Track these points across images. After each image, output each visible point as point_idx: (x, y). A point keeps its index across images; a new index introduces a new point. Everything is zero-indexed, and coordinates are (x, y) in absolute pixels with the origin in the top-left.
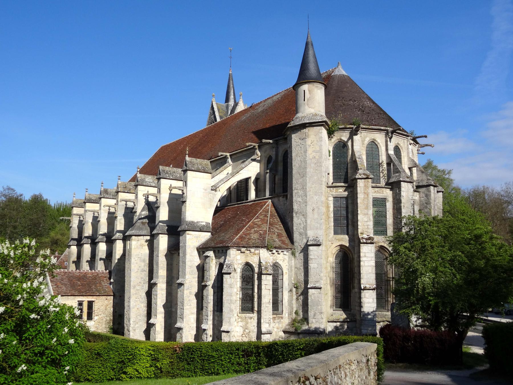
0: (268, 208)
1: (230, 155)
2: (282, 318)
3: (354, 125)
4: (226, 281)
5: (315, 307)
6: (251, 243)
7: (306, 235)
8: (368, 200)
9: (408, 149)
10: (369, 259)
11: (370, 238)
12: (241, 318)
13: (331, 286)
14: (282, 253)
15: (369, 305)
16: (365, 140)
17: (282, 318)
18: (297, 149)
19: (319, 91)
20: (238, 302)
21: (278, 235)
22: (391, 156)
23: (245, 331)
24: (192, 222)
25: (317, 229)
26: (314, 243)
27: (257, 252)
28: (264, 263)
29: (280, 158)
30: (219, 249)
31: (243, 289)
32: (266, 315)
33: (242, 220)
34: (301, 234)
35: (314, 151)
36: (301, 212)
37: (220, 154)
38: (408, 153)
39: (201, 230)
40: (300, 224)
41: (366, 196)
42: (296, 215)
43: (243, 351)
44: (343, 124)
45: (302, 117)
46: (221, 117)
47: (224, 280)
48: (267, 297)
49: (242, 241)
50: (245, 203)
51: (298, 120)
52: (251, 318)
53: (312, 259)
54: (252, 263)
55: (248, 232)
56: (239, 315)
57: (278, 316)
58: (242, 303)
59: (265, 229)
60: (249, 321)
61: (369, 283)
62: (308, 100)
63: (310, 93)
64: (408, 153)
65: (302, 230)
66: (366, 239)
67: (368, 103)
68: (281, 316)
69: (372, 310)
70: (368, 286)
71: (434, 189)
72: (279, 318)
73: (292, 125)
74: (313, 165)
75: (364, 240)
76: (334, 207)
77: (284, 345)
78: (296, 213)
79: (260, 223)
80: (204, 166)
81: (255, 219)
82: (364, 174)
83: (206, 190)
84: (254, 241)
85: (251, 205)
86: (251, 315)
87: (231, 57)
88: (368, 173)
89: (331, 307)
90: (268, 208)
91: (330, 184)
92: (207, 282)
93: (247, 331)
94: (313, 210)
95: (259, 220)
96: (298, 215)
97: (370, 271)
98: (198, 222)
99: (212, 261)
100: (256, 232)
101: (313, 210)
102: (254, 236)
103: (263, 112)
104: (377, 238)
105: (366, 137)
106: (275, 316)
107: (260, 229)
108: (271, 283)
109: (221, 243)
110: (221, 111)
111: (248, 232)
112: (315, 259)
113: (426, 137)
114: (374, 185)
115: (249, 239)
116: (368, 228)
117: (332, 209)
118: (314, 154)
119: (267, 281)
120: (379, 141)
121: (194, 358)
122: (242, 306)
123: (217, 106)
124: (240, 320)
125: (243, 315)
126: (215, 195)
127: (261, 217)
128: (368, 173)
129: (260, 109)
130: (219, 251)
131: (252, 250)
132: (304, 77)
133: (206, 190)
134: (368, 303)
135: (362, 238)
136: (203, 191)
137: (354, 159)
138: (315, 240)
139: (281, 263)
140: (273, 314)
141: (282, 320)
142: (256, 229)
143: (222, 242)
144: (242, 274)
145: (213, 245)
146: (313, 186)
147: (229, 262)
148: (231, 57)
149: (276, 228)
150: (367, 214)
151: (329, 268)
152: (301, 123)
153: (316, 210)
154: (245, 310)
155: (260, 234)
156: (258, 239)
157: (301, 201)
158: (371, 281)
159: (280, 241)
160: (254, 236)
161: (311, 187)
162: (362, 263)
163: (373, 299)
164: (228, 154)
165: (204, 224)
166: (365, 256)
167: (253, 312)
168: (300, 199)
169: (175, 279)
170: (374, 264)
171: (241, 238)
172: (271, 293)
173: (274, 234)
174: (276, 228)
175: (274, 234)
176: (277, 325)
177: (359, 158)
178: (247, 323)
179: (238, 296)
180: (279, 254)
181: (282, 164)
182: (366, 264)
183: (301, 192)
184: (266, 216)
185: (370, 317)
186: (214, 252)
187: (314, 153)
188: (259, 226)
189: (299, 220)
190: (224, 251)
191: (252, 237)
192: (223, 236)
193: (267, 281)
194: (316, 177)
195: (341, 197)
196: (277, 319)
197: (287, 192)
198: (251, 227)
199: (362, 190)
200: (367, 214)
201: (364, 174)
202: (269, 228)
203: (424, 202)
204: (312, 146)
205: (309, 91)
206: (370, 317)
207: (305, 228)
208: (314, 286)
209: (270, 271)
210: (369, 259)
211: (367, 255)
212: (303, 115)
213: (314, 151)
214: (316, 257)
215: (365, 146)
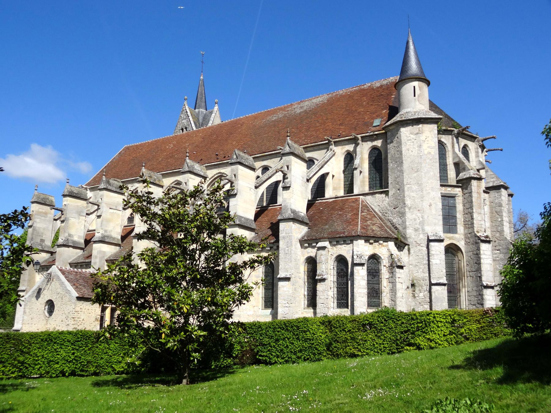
4: (358, 272)
5: (439, 304)
7: (423, 230)
10: (487, 257)
25: (435, 225)
26: (436, 238)
27: (385, 244)
30: (338, 239)
31: (369, 283)
34: (416, 230)
35: (429, 147)
36: (415, 208)
40: (415, 220)
42: (409, 209)
44: (446, 126)
45: (415, 112)
48: (400, 291)
50: (322, 200)
51: (410, 114)
53: (433, 255)
54: (380, 255)
62: (419, 96)
65: (418, 226)
74: (428, 161)
75: (484, 238)
78: (410, 209)
87: (202, 62)
94: (430, 205)
96: (411, 210)
97: (489, 269)
101: (430, 205)
112: (437, 254)
113: (501, 150)
118: (429, 150)
120: (470, 147)
131: (381, 242)
136: (301, 179)
148: (202, 62)
150: (480, 213)
153: (433, 206)
154: (371, 306)
157: (415, 195)
161: (428, 183)
162: (482, 261)
166: (484, 254)
168: (412, 194)
183: (415, 187)
186: (330, 242)
189: (414, 216)
194: (432, 173)
197: (388, 188)
200: (480, 213)
204: (426, 142)
205: (419, 87)
207: (422, 223)
208: (438, 282)
210: (487, 257)
211: (485, 252)
213: (429, 147)
214: (438, 253)
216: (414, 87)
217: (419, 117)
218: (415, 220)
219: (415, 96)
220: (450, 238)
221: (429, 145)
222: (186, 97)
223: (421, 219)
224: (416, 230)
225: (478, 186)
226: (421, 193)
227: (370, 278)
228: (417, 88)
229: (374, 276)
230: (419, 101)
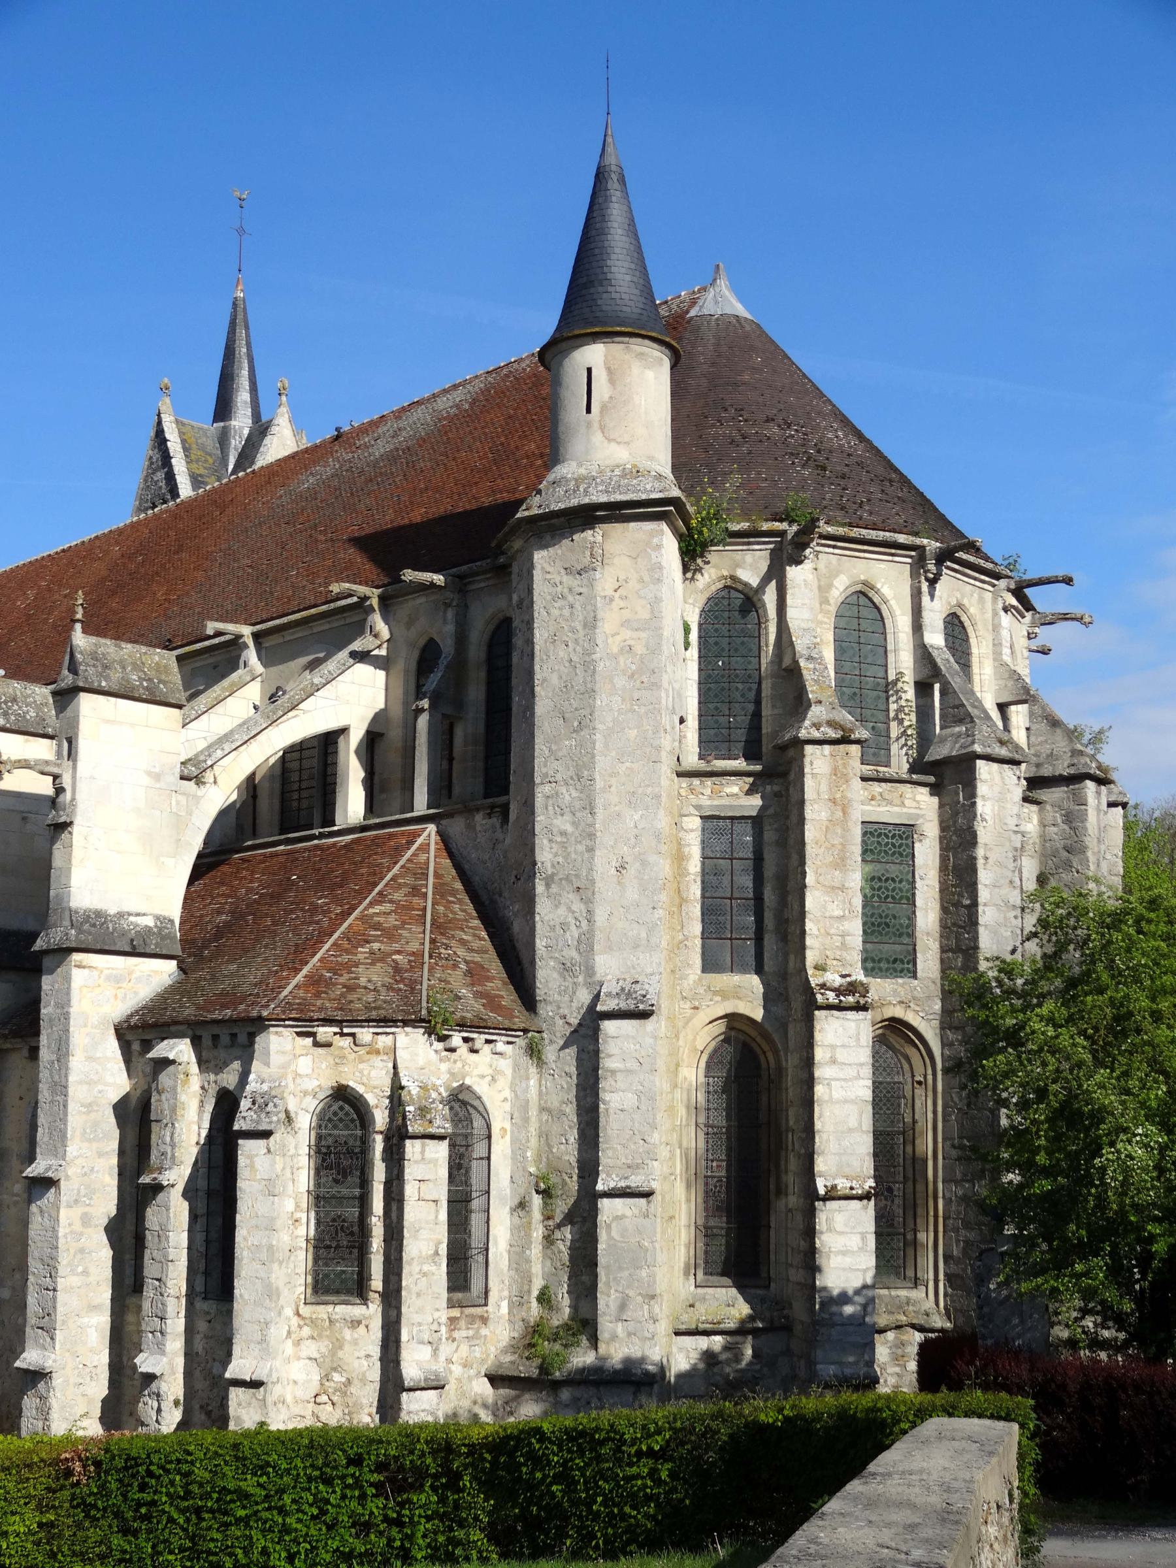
0: (423, 857)
1: (256, 636)
2: (484, 1320)
3: (791, 522)
5: (626, 1274)
6: (358, 1003)
7: (590, 971)
8: (846, 830)
9: (996, 628)
10: (851, 1072)
11: (852, 988)
12: (313, 1322)
13: (688, 1186)
14: (487, 1048)
15: (848, 1260)
16: (830, 586)
17: (484, 1320)
18: (556, 612)
19: (650, 374)
20: (302, 1255)
21: (469, 973)
22: (935, 653)
23: (327, 1377)
24: (98, 914)
25: (636, 947)
27: (384, 1041)
28: (415, 1091)
29: (476, 651)
30: (216, 1030)
31: (319, 1199)
32: (420, 1310)
33: (315, 909)
34: (566, 968)
35: (626, 624)
36: (567, 878)
37: (211, 627)
38: (997, 645)
39: (136, 947)
40: (564, 926)
41: (839, 814)
42: (548, 886)
43: (381, 1467)
44: (745, 515)
45: (578, 480)
46: (196, 481)
47: (242, 1161)
48: (424, 1234)
49: (317, 995)
50: (322, 836)
51: (560, 491)
52: (355, 1323)
53: (613, 1072)
54: (361, 1089)
55: (345, 958)
56: (305, 1311)
57: (469, 1311)
58: (316, 1259)
59: (414, 946)
60: (348, 1334)
61: (847, 1171)
62: (604, 408)
63: (612, 382)
64: (997, 645)
65: (574, 954)
66: (838, 991)
67: (837, 437)
68: (478, 1311)
69: (858, 1283)
70: (843, 1184)
71: (1098, 793)
72: (472, 1319)
73: (535, 511)
74: (620, 682)
76: (705, 857)
77: (571, 1439)
79: (392, 920)
80: (152, 674)
81: (371, 904)
82: (831, 724)
83: (157, 777)
84: (370, 997)
85: (347, 847)
86: (357, 1311)
87: (241, 231)
88: (846, 717)
89: (686, 1273)
90: (423, 857)
91: (692, 759)
92: (161, 1170)
93: (336, 1377)
95: (387, 907)
96: (554, 889)
97: (853, 1122)
98: (121, 915)
99: (186, 1082)
100: (376, 958)
102: (372, 976)
103: (391, 457)
104: (882, 989)
105: (838, 573)
106: (456, 1313)
107: (396, 946)
108: (443, 1172)
109: (224, 1006)
110: (196, 453)
111: (345, 958)
112: (629, 1072)
113: (1068, 581)
114: (867, 770)
115: (350, 988)
116: (844, 946)
117: (694, 865)
118: (627, 634)
119: (427, 1164)
120: (886, 591)
121: (153, 1503)
122: (316, 1274)
123: (181, 433)
124: (306, 1331)
125: (323, 1311)
126: (197, 799)
127: (397, 896)
128: (846, 717)
129: (380, 449)
130: (215, 1038)
131: (365, 1034)
132: (586, 313)
133: (157, 777)
134: (844, 1253)
135: (823, 986)
136: (147, 781)
137: (787, 662)
138: (629, 994)
139: (481, 1088)
140: (451, 1305)
141: (484, 1331)
142: (376, 946)
143: (230, 999)
144: (319, 1138)
145: (189, 1012)
146: (622, 769)
147: (265, 1087)
148: (241, 231)
149: (463, 942)
150: (842, 888)
151: (682, 1111)
152: (574, 502)
153: (632, 871)
154: (327, 1291)
155: (397, 969)
156: (389, 988)
157: (569, 828)
158: (856, 1163)
159: (478, 995)
160: (372, 976)
161: (614, 774)
162: (819, 1090)
163: (864, 1238)
164: (246, 631)
165: (149, 922)
166: (833, 1061)
167: (365, 1300)
168: (564, 823)
169: (15, 1163)
170: (868, 1094)
171: (314, 981)
172: (443, 1216)
173: (455, 966)
174: (463, 942)
175: (455, 966)
176: (464, 1349)
177: (810, 658)
178: (338, 1344)
179: (302, 1231)
180: (474, 1051)
181: (483, 674)
182: (837, 1094)
183: (568, 795)
184: (416, 891)
185: (848, 1310)
186: (196, 1043)
187: (621, 632)
188: (390, 934)
189: (562, 911)
190: (242, 1039)
191: (363, 981)
192: (232, 975)
193: (427, 1164)
194: (633, 733)
195: (732, 818)
196: (463, 1323)
197: (506, 791)
198: (356, 939)
199: (824, 787)
200: (842, 888)
201: (831, 724)
202: (433, 941)
203: (1059, 845)
205: (609, 371)
206: (848, 1310)
207: (586, 944)
208: (622, 1184)
209: (438, 1122)
210: (851, 1072)
211: (841, 1055)
212: (582, 471)
213: (626, 624)
214: (632, 1064)
215: (833, 609)
216: (589, 370)
217: (586, 501)
218: (564, 926)
219: (589, 410)
220: (724, 995)
221: (627, 614)
222: (166, 380)
223: (584, 923)
224: (566, 968)
225: (835, 771)
226: (590, 819)
227: (327, 1179)
228: (599, 376)
229: (344, 1173)
230: (602, 429)
